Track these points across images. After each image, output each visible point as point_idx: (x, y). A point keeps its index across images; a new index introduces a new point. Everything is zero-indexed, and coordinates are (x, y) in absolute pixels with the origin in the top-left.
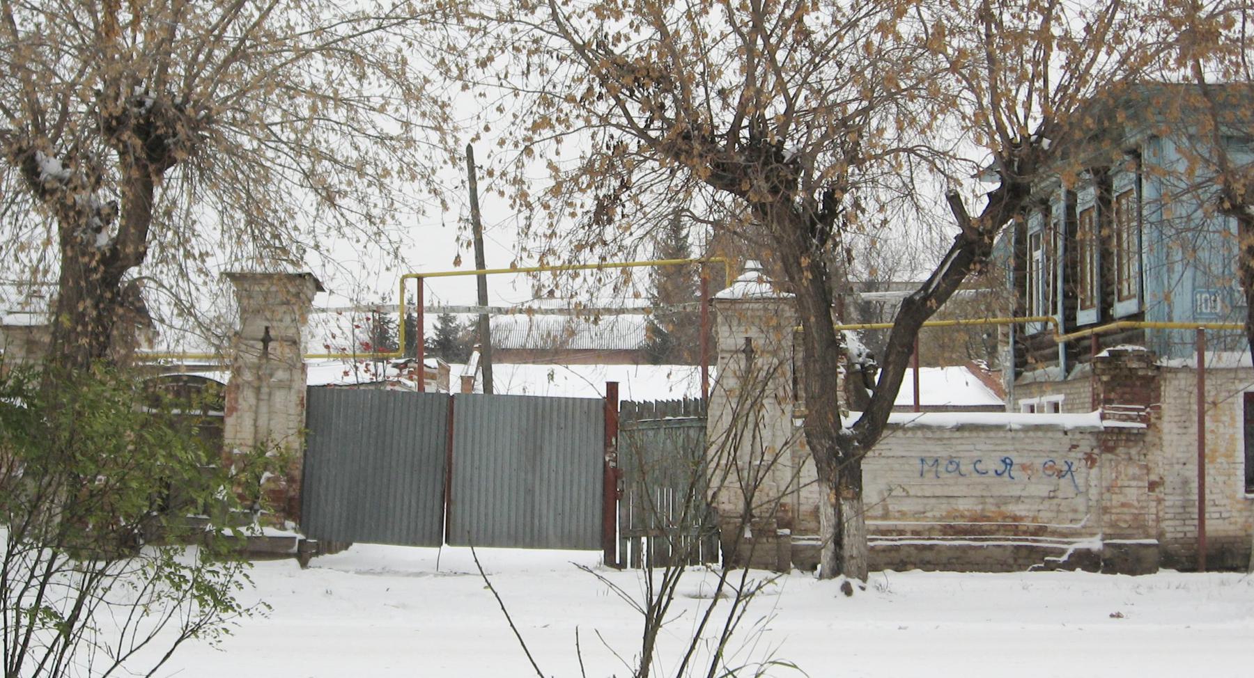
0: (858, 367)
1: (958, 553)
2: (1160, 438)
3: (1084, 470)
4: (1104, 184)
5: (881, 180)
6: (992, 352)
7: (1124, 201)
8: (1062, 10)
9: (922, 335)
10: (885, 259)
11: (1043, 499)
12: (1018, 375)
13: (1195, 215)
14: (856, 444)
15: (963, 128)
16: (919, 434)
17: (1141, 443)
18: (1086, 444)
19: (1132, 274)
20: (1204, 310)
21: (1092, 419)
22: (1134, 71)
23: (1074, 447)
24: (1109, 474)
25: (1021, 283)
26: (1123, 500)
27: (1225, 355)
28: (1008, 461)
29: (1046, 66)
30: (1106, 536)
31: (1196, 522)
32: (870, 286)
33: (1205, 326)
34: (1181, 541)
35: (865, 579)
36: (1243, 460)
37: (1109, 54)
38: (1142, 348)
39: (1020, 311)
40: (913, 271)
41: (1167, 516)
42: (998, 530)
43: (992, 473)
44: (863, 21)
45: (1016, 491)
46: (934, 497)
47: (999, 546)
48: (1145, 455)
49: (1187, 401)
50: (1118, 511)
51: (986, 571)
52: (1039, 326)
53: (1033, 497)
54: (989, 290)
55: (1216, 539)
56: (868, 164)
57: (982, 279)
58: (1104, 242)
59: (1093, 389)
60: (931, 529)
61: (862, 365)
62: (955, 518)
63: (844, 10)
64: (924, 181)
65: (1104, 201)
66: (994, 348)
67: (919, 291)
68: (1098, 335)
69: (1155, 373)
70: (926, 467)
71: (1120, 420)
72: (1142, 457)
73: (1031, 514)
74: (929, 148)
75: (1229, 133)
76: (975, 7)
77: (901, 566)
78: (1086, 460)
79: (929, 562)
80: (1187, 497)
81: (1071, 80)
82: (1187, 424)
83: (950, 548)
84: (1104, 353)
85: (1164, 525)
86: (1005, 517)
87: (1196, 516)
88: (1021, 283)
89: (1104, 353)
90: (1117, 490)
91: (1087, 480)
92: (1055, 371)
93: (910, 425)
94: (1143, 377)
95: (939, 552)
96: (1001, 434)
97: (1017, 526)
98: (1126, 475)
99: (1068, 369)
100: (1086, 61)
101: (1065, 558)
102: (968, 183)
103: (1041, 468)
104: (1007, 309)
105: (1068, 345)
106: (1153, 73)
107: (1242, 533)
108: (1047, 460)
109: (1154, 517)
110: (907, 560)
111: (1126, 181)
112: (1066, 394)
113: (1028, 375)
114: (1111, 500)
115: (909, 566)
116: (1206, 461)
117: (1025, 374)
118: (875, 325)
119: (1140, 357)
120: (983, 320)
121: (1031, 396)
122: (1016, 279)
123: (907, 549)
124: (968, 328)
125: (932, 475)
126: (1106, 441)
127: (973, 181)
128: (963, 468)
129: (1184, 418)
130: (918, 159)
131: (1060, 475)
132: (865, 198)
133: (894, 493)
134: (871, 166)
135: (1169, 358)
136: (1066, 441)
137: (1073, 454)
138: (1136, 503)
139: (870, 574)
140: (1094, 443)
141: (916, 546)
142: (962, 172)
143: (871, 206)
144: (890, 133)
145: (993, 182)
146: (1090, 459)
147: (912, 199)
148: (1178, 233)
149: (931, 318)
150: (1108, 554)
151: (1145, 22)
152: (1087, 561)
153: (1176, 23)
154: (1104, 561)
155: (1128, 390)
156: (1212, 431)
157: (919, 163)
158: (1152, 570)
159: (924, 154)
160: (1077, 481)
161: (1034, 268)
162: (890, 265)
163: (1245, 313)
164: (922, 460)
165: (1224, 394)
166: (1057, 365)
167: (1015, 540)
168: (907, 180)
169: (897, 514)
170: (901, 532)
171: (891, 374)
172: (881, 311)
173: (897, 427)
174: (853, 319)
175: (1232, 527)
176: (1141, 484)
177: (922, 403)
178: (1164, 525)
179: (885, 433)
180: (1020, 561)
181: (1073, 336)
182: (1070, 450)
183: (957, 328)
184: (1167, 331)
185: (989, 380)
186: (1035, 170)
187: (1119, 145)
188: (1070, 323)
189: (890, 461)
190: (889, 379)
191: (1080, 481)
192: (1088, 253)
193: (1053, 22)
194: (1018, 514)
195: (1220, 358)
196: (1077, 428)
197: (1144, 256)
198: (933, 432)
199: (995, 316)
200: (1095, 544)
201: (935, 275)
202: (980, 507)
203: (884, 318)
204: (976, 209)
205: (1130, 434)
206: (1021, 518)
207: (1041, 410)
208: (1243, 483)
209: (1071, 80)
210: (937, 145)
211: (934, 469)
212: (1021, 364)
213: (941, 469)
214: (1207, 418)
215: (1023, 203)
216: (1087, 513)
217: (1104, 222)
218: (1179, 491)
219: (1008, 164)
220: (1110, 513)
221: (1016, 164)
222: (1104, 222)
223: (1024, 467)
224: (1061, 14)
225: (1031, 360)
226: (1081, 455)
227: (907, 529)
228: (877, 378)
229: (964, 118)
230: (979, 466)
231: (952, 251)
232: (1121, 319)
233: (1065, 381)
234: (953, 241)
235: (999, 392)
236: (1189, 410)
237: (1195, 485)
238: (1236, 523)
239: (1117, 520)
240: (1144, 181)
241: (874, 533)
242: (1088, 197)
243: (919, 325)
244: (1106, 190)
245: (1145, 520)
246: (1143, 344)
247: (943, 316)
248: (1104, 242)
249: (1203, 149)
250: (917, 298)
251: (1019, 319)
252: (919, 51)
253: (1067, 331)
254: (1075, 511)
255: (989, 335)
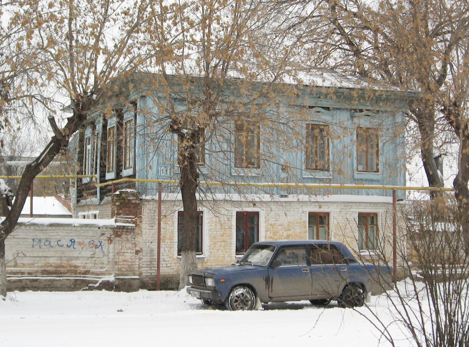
0: (4, 196)
1: (49, 283)
2: (141, 231)
3: (107, 245)
4: (120, 116)
5: (18, 110)
6: (67, 191)
7: (128, 124)
8: (104, 36)
9: (35, 181)
10: (19, 147)
11: (88, 258)
12: (78, 201)
13: (159, 132)
14: (2, 232)
15: (57, 87)
16: (32, 228)
17: (133, 233)
18: (109, 233)
19: (131, 157)
20: (162, 175)
21: (111, 222)
22: (136, 66)
23: (103, 234)
24: (118, 247)
25: (81, 159)
26: (124, 258)
27: (170, 195)
28: (73, 241)
29: (96, 62)
30: (116, 275)
31: (156, 268)
32: (12, 158)
33: (162, 182)
34: (149, 277)
35: (5, 295)
36: (177, 241)
37: (125, 58)
38: (134, 191)
39: (80, 172)
40: (32, 152)
41: (143, 266)
42: (68, 272)
43: (65, 246)
44: (13, 35)
45: (76, 254)
46: (38, 257)
47: (68, 279)
48: (134, 238)
49: (153, 215)
50: (122, 263)
51: (62, 291)
52: (88, 179)
53: (84, 257)
54: (66, 162)
55: (165, 276)
56: (12, 101)
57: (63, 157)
58: (119, 142)
59: (112, 208)
60: (37, 272)
61: (6, 195)
62: (48, 267)
63: (5, 29)
64: (38, 111)
65: (120, 124)
66: (68, 189)
67: (34, 162)
68: (115, 184)
69: (140, 202)
70: (35, 243)
71: (123, 222)
72: (133, 239)
73: (83, 265)
74: (41, 96)
75: (175, 97)
76: (65, 32)
77: (23, 289)
78: (108, 240)
79: (36, 287)
80: (152, 257)
81: (107, 69)
82: (153, 225)
83: (45, 280)
84: (118, 193)
85: (141, 270)
86: (71, 266)
87: (156, 266)
88: (81, 159)
89: (118, 193)
90: (121, 254)
91: (108, 249)
92: (95, 200)
93: (28, 223)
94: (135, 203)
95: (40, 282)
96: (70, 228)
97: (76, 270)
98: (126, 247)
99: (101, 199)
100: (114, 60)
101: (98, 285)
102: (59, 113)
103: (88, 244)
104: (74, 171)
105: (101, 189)
106: (142, 68)
107: (176, 273)
108: (90, 240)
109: (138, 266)
110: (26, 286)
111: (130, 116)
112: (100, 210)
113: (83, 202)
114: (119, 259)
115: (26, 289)
116: (161, 241)
117: (81, 201)
118: (13, 177)
119: (133, 194)
120: (63, 176)
121: (84, 211)
122: (79, 158)
123: (25, 281)
124: (56, 179)
125: (37, 247)
126: (117, 232)
127: (61, 112)
128: (52, 244)
129: (152, 222)
130: (36, 100)
131: (96, 247)
132: (11, 117)
133: (20, 255)
134: (14, 103)
135: (146, 196)
136: (99, 232)
137: (102, 238)
138: (130, 260)
139: (7, 293)
140: (112, 233)
141: (29, 279)
142: (56, 107)
143: (13, 121)
144: (24, 88)
145: (70, 113)
146: (110, 240)
147: (33, 119)
148: (152, 139)
149: (39, 174)
150: (117, 283)
151: (141, 45)
152: (107, 286)
153: (154, 47)
154: (115, 286)
155: (127, 209)
156: (164, 228)
157: (36, 103)
158: (136, 290)
159: (39, 98)
160: (104, 250)
161: (87, 153)
162: (21, 149)
163: (179, 176)
164: (33, 240)
165: (170, 212)
166: (96, 197)
167: (75, 277)
168: (31, 110)
169: (21, 265)
170: (23, 273)
171: (20, 199)
172: (16, 170)
173: (21, 224)
174: (2, 174)
175: (172, 271)
176: (132, 251)
177: (34, 213)
178: (141, 270)
179: (16, 227)
180: (77, 286)
181: (104, 184)
182: (101, 236)
183: (52, 179)
184: (146, 183)
185: (65, 203)
186: (89, 109)
187: (127, 99)
188: (103, 178)
189: (18, 240)
190: (19, 201)
191: (105, 250)
192: (112, 147)
193: (100, 42)
194: (77, 265)
195: (168, 196)
196: (104, 226)
197: (136, 149)
198: (39, 227)
199: (69, 174)
200: (111, 278)
201: (42, 154)
202: (59, 262)
203: (17, 173)
204: (62, 124)
205: (128, 229)
206: (78, 267)
207: (88, 217)
208: (177, 251)
209: (107, 69)
210: (45, 95)
211: (39, 244)
212: (80, 196)
213: (42, 244)
214: (162, 222)
215: (83, 123)
216: (108, 265)
217: (119, 134)
218: (148, 255)
219: (77, 105)
220: (119, 265)
221: (81, 105)
222: (119, 134)
223: (80, 244)
224: (104, 39)
225: (85, 194)
226: (106, 238)
227: (25, 272)
228: (13, 202)
229: (58, 82)
230: (59, 243)
231: (50, 144)
232: (125, 177)
233: (100, 204)
234: (50, 139)
235: (69, 209)
236: (154, 219)
237: (156, 252)
238: (173, 269)
239: (121, 268)
240: (138, 116)
241: (10, 273)
242: (113, 122)
243: (34, 177)
244: (121, 119)
245: (133, 268)
246: (135, 188)
247: (45, 173)
248: (119, 142)
249: (164, 103)
250: (33, 165)
251: (79, 176)
252: (39, 51)
253: (101, 182)
254: (103, 263)
255: (65, 183)
